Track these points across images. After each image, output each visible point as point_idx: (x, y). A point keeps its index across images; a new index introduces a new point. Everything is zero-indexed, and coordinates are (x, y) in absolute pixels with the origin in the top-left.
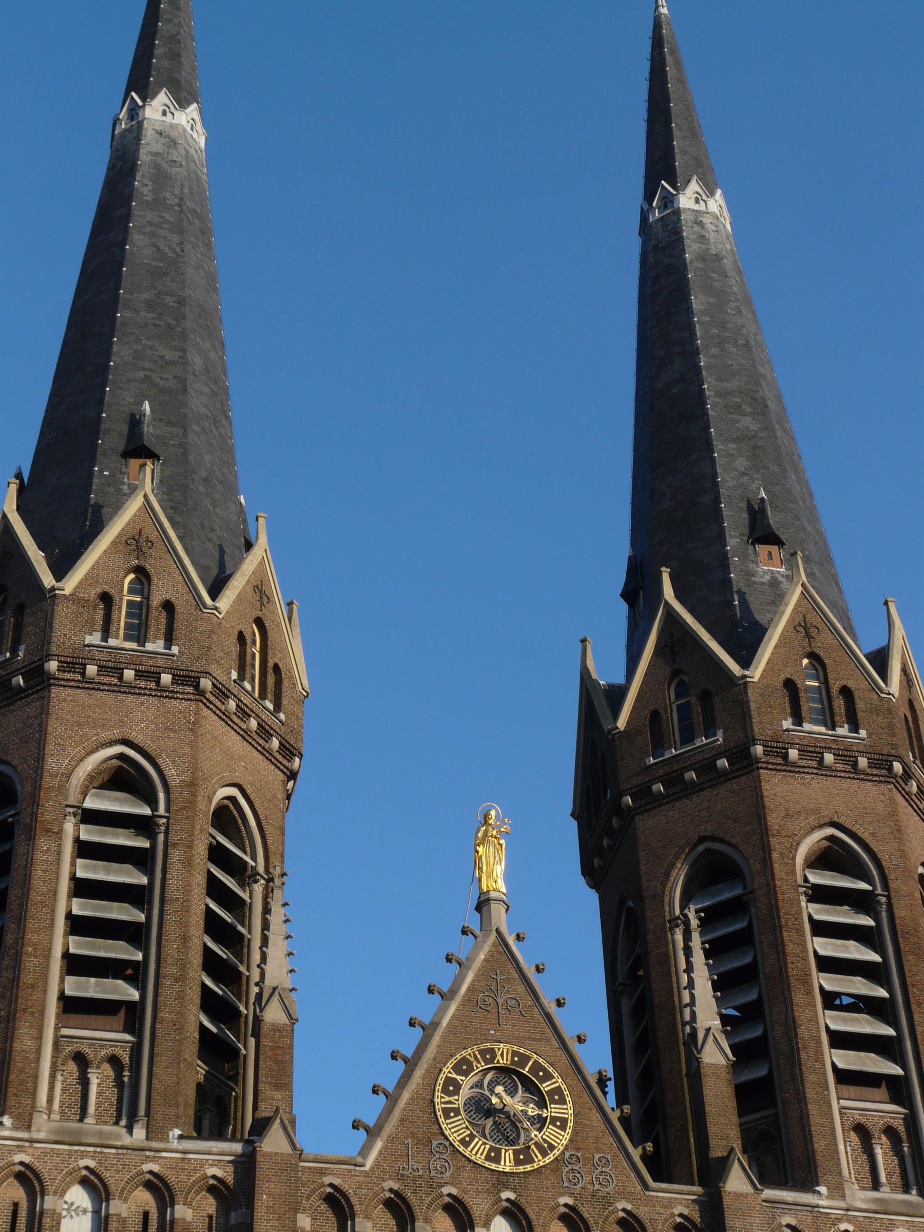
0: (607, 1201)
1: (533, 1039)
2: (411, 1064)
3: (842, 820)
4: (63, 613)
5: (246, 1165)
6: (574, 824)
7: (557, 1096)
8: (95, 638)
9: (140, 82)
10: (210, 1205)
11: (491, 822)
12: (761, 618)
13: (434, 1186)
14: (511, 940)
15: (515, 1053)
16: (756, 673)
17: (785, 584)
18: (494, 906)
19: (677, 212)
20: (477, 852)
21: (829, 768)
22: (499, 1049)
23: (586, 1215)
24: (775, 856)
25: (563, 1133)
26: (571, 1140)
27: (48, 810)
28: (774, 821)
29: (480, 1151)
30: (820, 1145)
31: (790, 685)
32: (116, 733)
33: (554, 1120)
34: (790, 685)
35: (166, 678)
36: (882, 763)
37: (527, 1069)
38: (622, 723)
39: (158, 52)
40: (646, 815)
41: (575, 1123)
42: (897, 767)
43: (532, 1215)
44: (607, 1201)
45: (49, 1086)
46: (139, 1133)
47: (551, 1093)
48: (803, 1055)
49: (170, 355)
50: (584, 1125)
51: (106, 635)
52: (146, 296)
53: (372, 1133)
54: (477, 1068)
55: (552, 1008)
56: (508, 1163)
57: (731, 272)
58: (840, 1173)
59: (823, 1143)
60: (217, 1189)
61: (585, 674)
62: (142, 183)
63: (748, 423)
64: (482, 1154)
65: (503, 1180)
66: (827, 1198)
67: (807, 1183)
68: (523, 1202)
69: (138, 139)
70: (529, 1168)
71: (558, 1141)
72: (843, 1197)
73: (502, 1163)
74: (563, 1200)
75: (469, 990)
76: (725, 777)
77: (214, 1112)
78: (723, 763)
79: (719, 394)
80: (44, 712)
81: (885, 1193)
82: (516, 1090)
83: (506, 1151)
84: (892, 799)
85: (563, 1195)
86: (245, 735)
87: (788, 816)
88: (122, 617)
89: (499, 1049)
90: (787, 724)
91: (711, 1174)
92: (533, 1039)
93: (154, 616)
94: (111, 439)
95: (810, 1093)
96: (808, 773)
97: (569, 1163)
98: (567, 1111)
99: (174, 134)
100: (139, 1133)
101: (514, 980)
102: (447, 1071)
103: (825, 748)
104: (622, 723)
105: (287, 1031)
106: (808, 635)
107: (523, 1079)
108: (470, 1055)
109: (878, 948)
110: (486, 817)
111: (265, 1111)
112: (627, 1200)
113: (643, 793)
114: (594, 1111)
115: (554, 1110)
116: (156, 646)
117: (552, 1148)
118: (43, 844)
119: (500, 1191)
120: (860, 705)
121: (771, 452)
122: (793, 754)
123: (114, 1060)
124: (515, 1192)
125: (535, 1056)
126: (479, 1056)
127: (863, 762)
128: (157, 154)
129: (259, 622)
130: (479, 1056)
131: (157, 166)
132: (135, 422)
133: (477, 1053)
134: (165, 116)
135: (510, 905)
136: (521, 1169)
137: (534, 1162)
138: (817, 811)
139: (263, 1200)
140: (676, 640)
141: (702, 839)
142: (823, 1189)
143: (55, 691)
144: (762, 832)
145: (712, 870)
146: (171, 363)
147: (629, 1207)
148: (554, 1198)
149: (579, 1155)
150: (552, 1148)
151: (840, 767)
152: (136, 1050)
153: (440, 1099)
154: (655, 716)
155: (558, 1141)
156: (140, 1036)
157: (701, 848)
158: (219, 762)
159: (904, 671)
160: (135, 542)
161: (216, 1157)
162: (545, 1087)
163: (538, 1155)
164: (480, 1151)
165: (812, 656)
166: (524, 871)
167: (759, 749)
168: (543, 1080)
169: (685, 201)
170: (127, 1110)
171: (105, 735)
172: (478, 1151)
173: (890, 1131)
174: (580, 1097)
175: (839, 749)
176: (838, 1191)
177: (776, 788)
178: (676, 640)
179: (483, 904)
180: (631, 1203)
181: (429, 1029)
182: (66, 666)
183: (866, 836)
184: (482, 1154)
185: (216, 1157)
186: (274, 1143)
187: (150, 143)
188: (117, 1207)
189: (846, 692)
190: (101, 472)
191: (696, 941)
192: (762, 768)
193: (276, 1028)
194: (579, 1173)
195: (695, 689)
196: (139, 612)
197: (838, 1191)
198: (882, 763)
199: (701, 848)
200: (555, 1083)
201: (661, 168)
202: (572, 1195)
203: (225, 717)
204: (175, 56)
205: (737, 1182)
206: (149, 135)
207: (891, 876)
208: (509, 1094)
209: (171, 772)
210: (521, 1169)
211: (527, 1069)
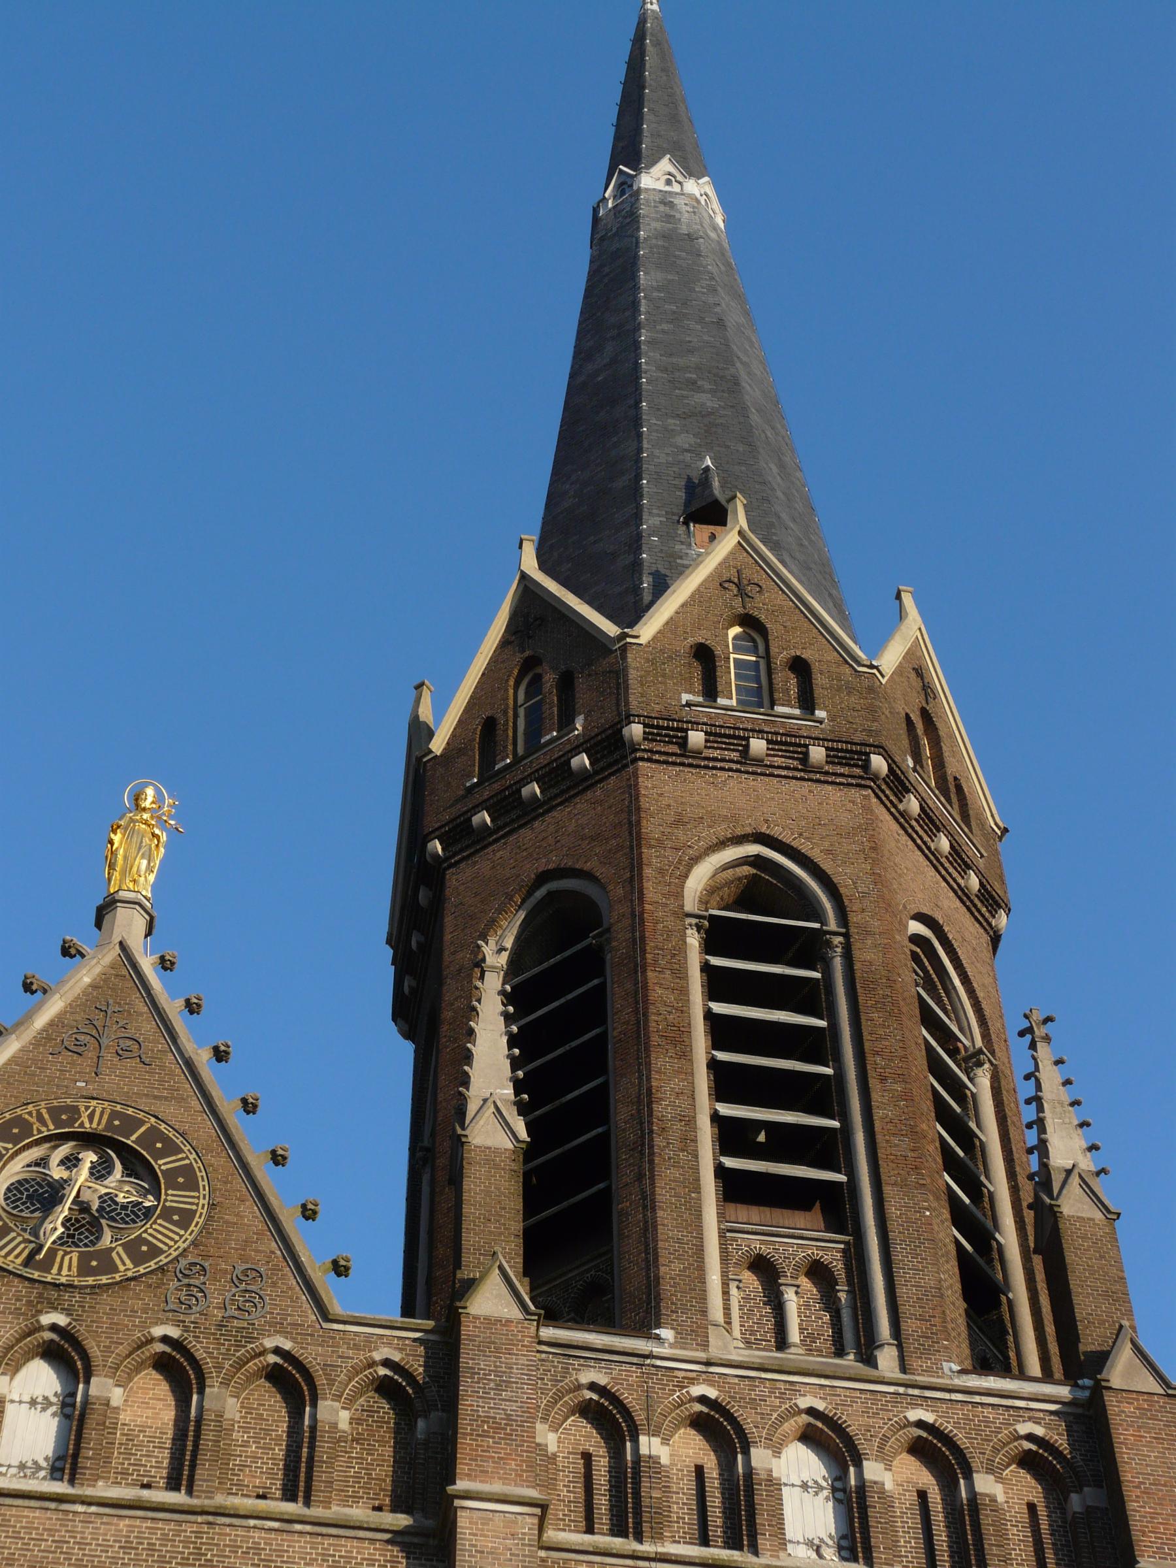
1: (155, 1097)
3: (776, 832)
6: (390, 952)
7: (187, 1179)
11: (147, 804)
14: (147, 964)
15: (114, 1115)
16: (647, 630)
18: (122, 912)
20: (111, 842)
21: (758, 761)
22: (87, 1108)
23: (200, 1354)
24: (648, 872)
25: (182, 1232)
26: (194, 1243)
28: (651, 828)
29: (16, 1252)
30: (670, 1269)
33: (167, 1214)
37: (133, 1138)
40: (463, 865)
41: (210, 1218)
42: (878, 763)
43: (94, 1351)
47: (170, 1174)
48: (659, 1141)
50: (227, 1222)
54: (40, 1132)
55: (203, 1058)
56: (65, 1272)
58: (704, 1312)
59: (677, 1266)
64: (17, 1257)
66: (671, 1346)
68: (81, 1331)
70: (104, 1280)
71: (171, 1243)
72: (705, 1346)
73: (55, 1270)
74: (158, 1331)
75: (51, 1024)
76: (585, 781)
82: (110, 1170)
83: (66, 1253)
84: (867, 809)
85: (159, 1322)
87: (679, 822)
89: (87, 1108)
92: (155, 1097)
95: (664, 1194)
96: (722, 769)
97: (186, 1276)
98: (199, 1202)
101: (141, 1014)
103: (753, 730)
106: (742, 593)
107: (125, 1152)
108: (30, 1114)
110: (137, 798)
112: (286, 1334)
114: (249, 1203)
115: (172, 1198)
117: (155, 1252)
119: (40, 1312)
122: (696, 738)
124: (68, 1315)
125: (153, 1120)
126: (46, 1116)
127: (817, 753)
130: (46, 1116)
133: (44, 1111)
135: (154, 914)
136: (90, 1280)
137: (117, 1270)
138: (734, 819)
141: (543, 878)
142: (666, 1333)
147: (287, 1345)
148: (144, 1325)
149: (206, 1265)
150: (155, 1252)
151: (778, 761)
154: (490, 725)
155: (171, 1243)
157: (540, 893)
162: (162, 1165)
163: (128, 1262)
164: (16, 1252)
165: (749, 622)
167: (636, 730)
168: (159, 1154)
173: (817, 1271)
174: (226, 1183)
175: (776, 733)
176: (697, 1333)
180: (294, 1340)
183: (816, 855)
184: (17, 1257)
189: (800, 667)
192: (642, 759)
194: (202, 1291)
199: (540, 893)
200: (183, 1159)
202: (178, 1323)
207: (853, 906)
208: (92, 1174)
210: (90, 1280)
211: (133, 1138)
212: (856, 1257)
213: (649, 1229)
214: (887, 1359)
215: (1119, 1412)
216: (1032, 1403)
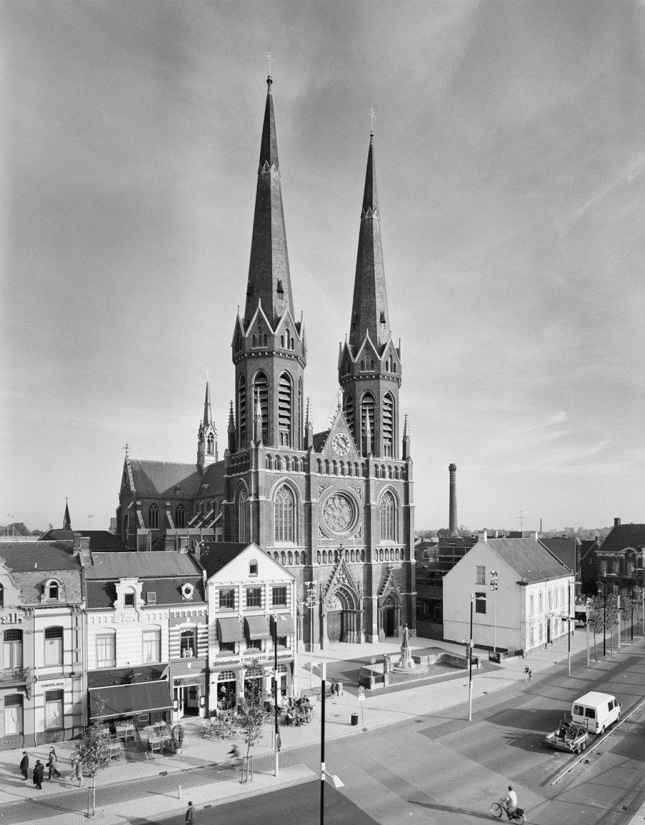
46: (292, 449)
51: (283, 347)
60: (303, 458)
100: (292, 449)
113: (358, 377)
123: (286, 434)
143: (276, 359)
152: (290, 433)
154: (362, 361)
156: (290, 430)
177: (382, 382)
182: (277, 353)
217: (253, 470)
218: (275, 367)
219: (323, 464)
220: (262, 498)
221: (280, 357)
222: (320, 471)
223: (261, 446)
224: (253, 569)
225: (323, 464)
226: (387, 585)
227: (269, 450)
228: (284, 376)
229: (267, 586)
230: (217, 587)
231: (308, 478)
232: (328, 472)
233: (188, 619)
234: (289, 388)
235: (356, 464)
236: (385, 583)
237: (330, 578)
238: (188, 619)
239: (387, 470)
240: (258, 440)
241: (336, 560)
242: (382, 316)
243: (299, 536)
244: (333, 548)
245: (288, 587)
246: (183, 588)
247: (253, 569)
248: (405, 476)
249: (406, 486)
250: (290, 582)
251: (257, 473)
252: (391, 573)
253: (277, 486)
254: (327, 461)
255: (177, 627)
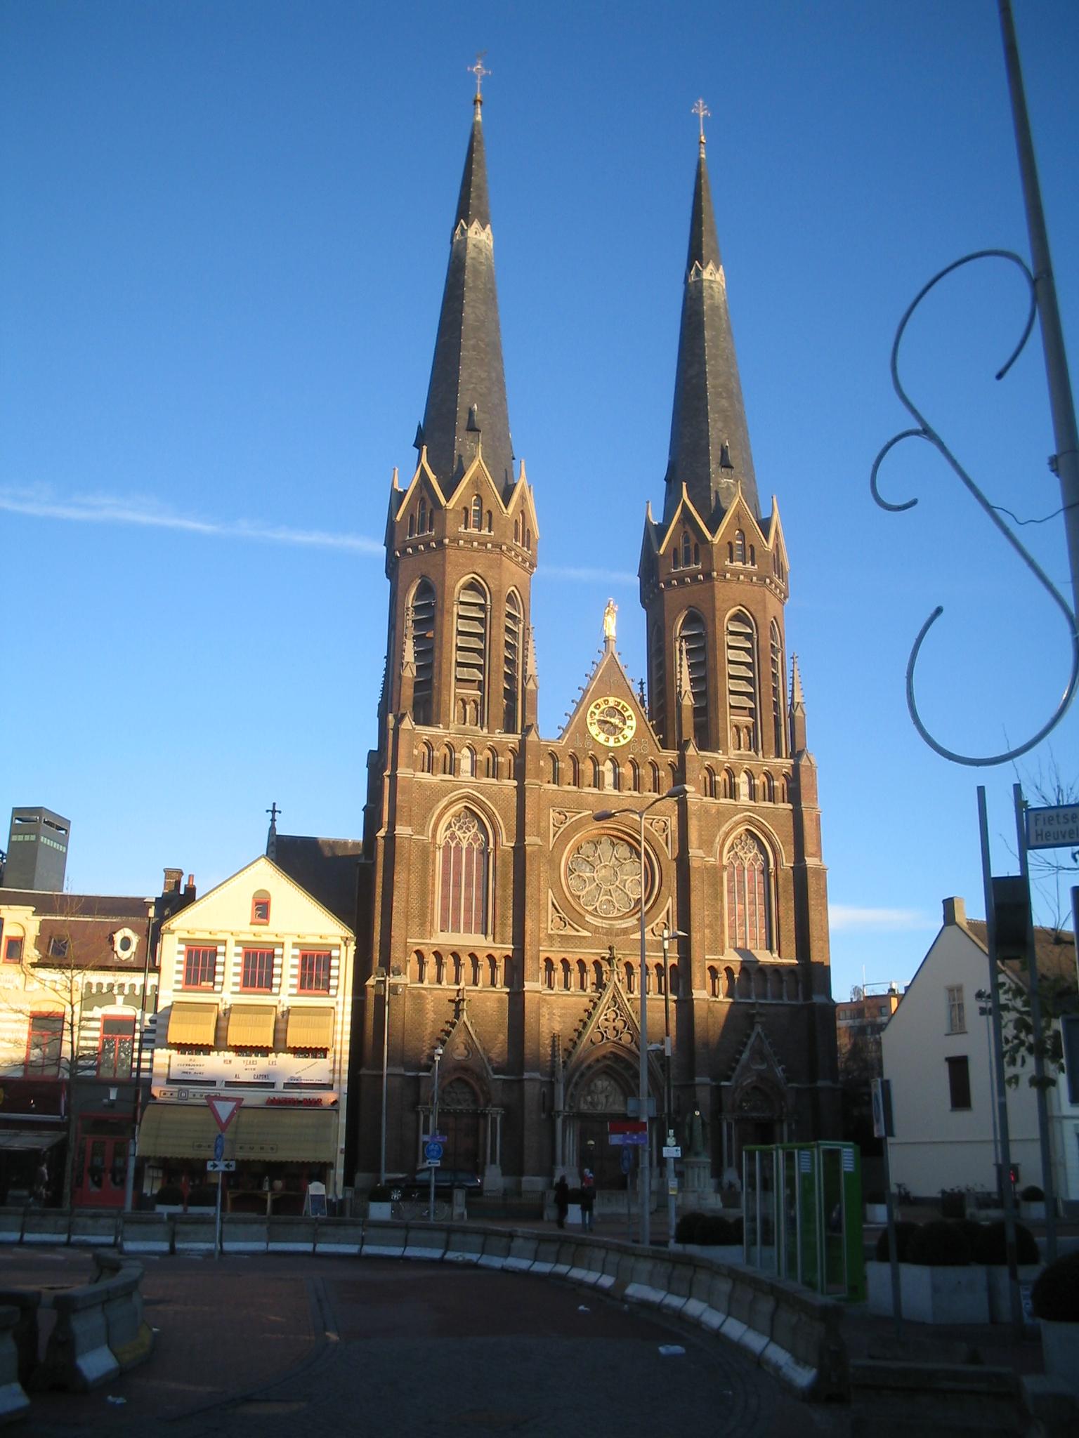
0: (646, 756)
2: (579, 705)
4: (450, 516)
5: (523, 743)
8: (462, 529)
9: (464, 213)
10: (510, 756)
12: (723, 505)
13: (587, 750)
17: (733, 489)
19: (702, 281)
27: (447, 605)
28: (718, 604)
30: (721, 735)
31: (730, 543)
32: (471, 569)
34: (730, 543)
35: (489, 546)
36: (762, 579)
38: (661, 552)
39: (473, 195)
44: (646, 756)
45: (454, 711)
46: (485, 730)
49: (484, 375)
52: (472, 342)
53: (565, 731)
57: (724, 317)
61: (647, 521)
62: (468, 277)
63: (724, 403)
65: (609, 749)
67: (715, 750)
69: (465, 248)
77: (510, 729)
78: (701, 577)
79: (713, 387)
80: (444, 558)
81: (743, 751)
86: (517, 564)
88: (472, 518)
90: (727, 563)
91: (682, 747)
93: (485, 518)
94: (461, 423)
99: (481, 245)
100: (485, 730)
102: (592, 708)
104: (661, 552)
105: (535, 693)
109: (752, 656)
111: (528, 723)
113: (668, 584)
116: (485, 532)
118: (447, 617)
120: (756, 553)
121: (735, 420)
122: (728, 575)
127: (755, 579)
128: (473, 258)
129: (522, 512)
131: (474, 266)
132: (471, 413)
134: (480, 236)
139: (529, 757)
140: (687, 517)
144: (713, 608)
145: (693, 619)
146: (483, 380)
152: (483, 698)
153: (589, 720)
154: (675, 550)
158: (510, 576)
159: (777, 532)
160: (476, 483)
161: (513, 739)
162: (626, 714)
166: (620, 625)
169: (706, 275)
170: (480, 720)
171: (467, 570)
172: (601, 738)
176: (726, 753)
178: (687, 517)
179: (606, 641)
181: (586, 692)
185: (513, 739)
186: (532, 737)
187: (471, 252)
188: (479, 757)
190: (458, 439)
191: (685, 663)
193: (531, 691)
195: (695, 548)
196: (479, 513)
197: (726, 753)
198: (762, 579)
201: (696, 254)
203: (510, 558)
204: (479, 197)
205: (691, 751)
206: (470, 246)
209: (492, 586)
212: (755, 724)
213: (717, 724)
214: (760, 753)
215: (802, 769)
216: (786, 763)
217: (388, 773)
218: (449, 569)
219: (565, 765)
220: (402, 830)
221: (460, 548)
222: (556, 781)
223: (407, 723)
224: (262, 908)
225: (565, 765)
226: (745, 1056)
227: (426, 731)
228: (472, 586)
229: (288, 946)
230: (182, 941)
231: (521, 791)
232: (576, 781)
233: (120, 999)
234: (482, 607)
235: (655, 766)
236: (741, 1053)
237: (580, 1026)
238: (120, 999)
239: (742, 780)
240: (402, 711)
241: (600, 985)
242: (724, 452)
243: (498, 922)
244: (589, 954)
245: (335, 953)
246: (118, 937)
247: (262, 908)
248: (794, 793)
249: (797, 816)
250: (338, 941)
251: (393, 777)
252: (758, 1028)
253: (446, 807)
254: (575, 759)
255: (98, 1012)
